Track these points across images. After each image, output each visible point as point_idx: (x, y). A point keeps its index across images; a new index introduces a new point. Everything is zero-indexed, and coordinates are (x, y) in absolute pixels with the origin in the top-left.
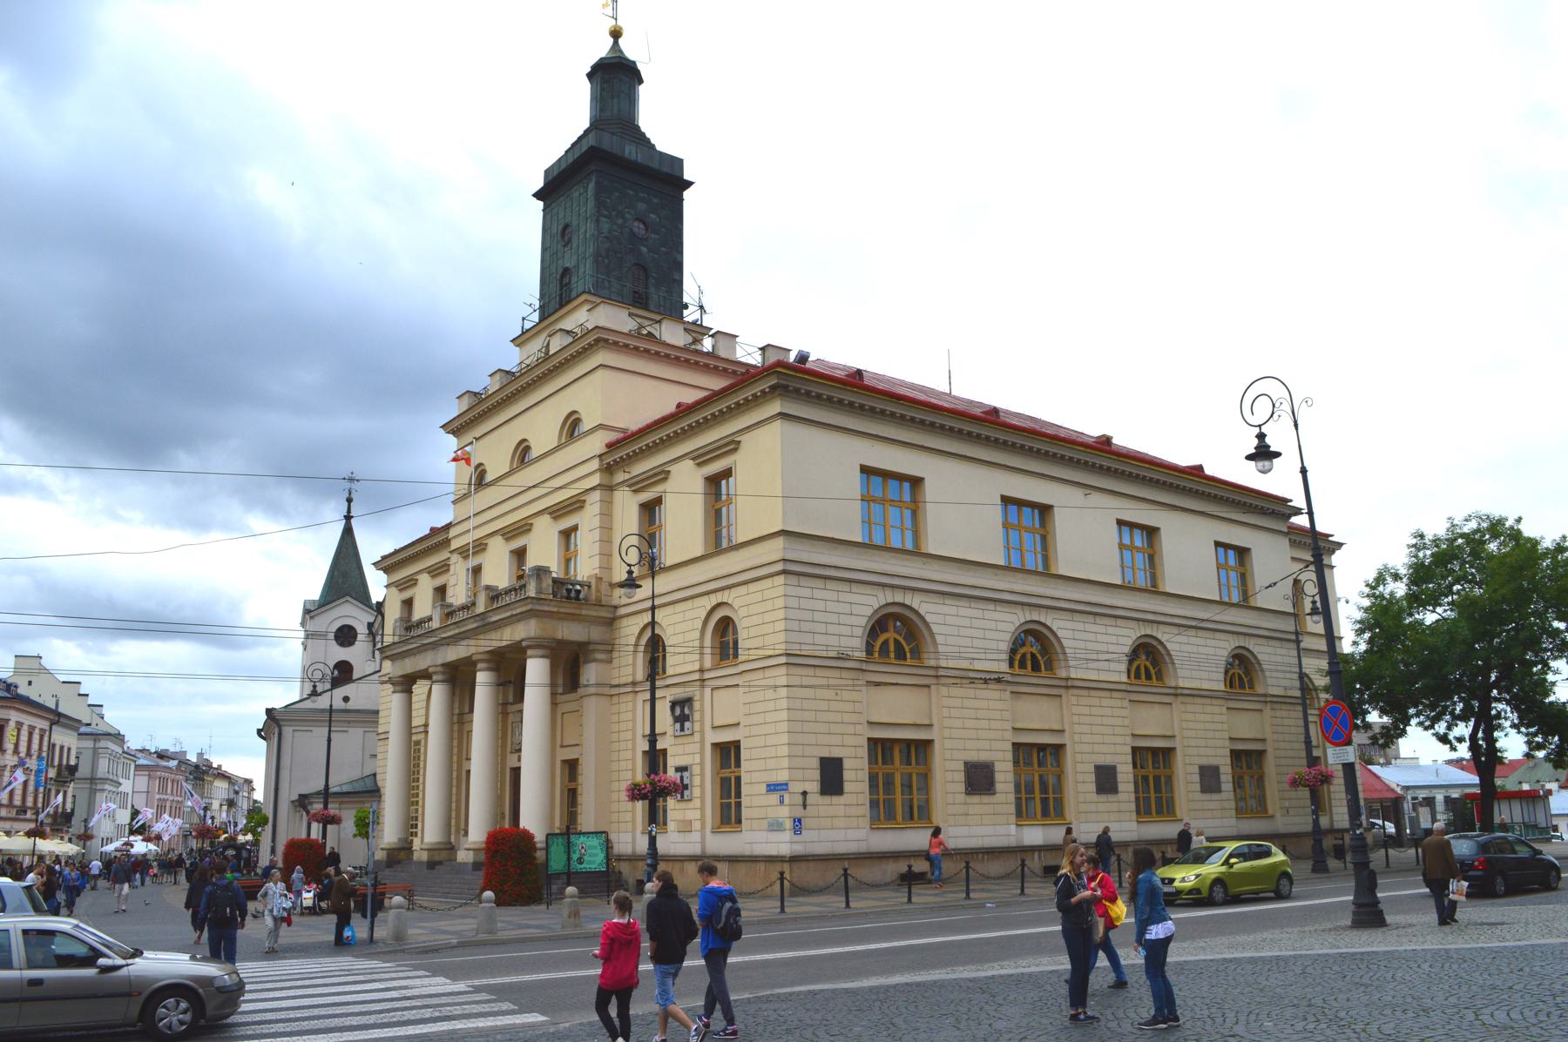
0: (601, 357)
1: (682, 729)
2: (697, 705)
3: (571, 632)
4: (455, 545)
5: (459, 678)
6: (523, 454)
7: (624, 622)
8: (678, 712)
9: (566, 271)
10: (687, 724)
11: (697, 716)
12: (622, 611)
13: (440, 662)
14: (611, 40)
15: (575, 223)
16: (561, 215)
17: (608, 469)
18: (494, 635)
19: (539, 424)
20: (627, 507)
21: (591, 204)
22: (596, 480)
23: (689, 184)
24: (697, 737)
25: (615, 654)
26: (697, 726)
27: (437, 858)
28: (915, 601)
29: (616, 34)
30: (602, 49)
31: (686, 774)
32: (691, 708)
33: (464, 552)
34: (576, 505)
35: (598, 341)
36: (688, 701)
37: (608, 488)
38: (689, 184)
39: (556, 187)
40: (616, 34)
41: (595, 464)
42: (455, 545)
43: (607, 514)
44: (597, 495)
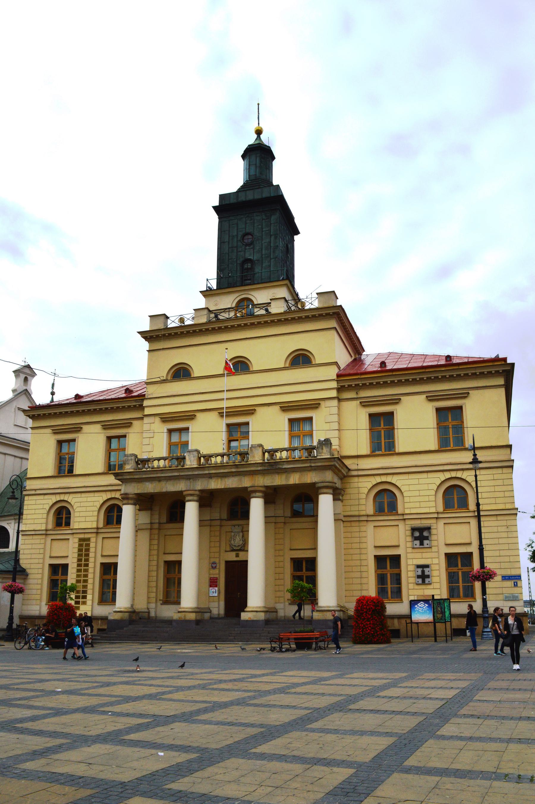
1: (422, 544)
2: (433, 531)
4: (147, 411)
8: (417, 534)
10: (426, 542)
11: (433, 537)
13: (199, 488)
14: (256, 136)
15: (257, 233)
17: (339, 390)
18: (284, 476)
19: (267, 350)
22: (334, 394)
24: (434, 549)
25: (344, 497)
26: (434, 543)
29: (259, 132)
30: (252, 139)
31: (426, 570)
32: (430, 533)
33: (165, 418)
34: (315, 405)
35: (334, 313)
36: (429, 529)
39: (228, 208)
40: (259, 132)
42: (147, 411)
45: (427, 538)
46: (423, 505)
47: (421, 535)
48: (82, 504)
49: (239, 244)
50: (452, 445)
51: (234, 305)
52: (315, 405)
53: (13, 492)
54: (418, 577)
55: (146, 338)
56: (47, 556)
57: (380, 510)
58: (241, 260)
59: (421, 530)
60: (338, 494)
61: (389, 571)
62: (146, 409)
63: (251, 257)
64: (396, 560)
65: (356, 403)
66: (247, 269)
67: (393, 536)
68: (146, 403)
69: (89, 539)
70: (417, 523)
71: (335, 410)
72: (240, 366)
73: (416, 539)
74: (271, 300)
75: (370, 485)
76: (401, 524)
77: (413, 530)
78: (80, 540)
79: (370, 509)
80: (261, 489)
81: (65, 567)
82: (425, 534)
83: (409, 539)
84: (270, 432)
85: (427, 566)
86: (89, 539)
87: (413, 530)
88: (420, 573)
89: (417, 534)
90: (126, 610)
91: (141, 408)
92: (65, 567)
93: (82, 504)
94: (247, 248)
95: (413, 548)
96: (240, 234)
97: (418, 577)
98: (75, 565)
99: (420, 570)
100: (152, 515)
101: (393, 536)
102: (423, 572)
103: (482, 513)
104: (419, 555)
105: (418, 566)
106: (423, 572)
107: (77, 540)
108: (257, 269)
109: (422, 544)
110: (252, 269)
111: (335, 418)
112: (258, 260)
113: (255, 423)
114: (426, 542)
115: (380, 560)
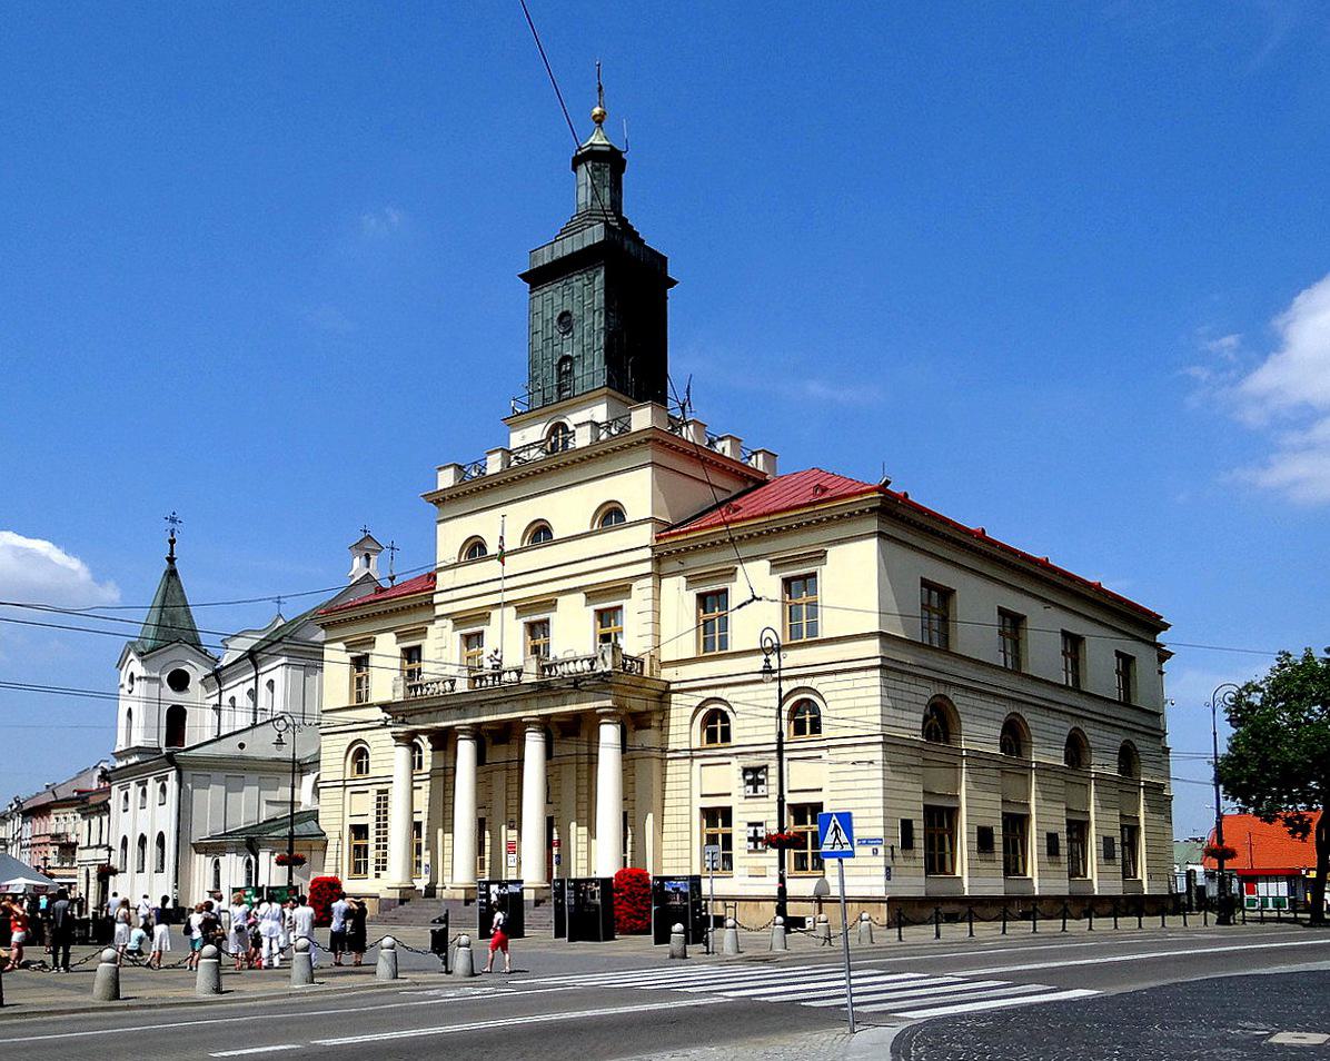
0: (647, 455)
1: (755, 790)
3: (636, 704)
4: (439, 610)
5: (498, 743)
6: (540, 533)
7: (674, 696)
9: (566, 359)
12: (673, 687)
15: (576, 313)
16: (558, 301)
17: (658, 560)
19: (569, 508)
20: (679, 598)
21: (599, 298)
22: (647, 567)
23: (672, 283)
27: (472, 896)
28: (950, 693)
32: (766, 774)
33: (459, 620)
34: (623, 589)
36: (766, 767)
37: (658, 576)
38: (672, 283)
41: (647, 553)
42: (439, 610)
43: (657, 599)
44: (649, 581)
45: (762, 782)
46: (760, 731)
47: (754, 776)
48: (380, 744)
49: (555, 331)
50: (805, 636)
51: (544, 437)
52: (623, 589)
53: (280, 736)
54: (750, 839)
55: (437, 503)
56: (347, 813)
57: (712, 737)
58: (558, 359)
59: (756, 770)
60: (632, 723)
61: (720, 830)
62: (437, 608)
63: (570, 353)
64: (726, 814)
65: (682, 580)
66: (566, 372)
67: (724, 780)
68: (437, 598)
69: (386, 791)
70: (753, 762)
71: (649, 593)
72: (540, 533)
73: (749, 783)
74: (575, 425)
75: (697, 702)
76: (733, 760)
77: (746, 771)
78: (379, 792)
79: (697, 738)
80: (537, 719)
81: (365, 827)
82: (761, 777)
83: (742, 783)
84: (573, 635)
85: (761, 824)
86: (386, 791)
87: (746, 771)
88: (752, 835)
89: (749, 777)
90: (396, 886)
91: (432, 605)
92: (365, 827)
93: (380, 744)
94: (566, 337)
95: (746, 797)
96: (558, 314)
97: (750, 839)
98: (374, 826)
99: (752, 829)
100: (445, 754)
101: (724, 780)
102: (756, 832)
103: (786, 747)
104: (753, 807)
105: (750, 824)
106: (756, 832)
107: (375, 792)
108: (578, 373)
109: (755, 790)
110: (571, 372)
111: (649, 605)
112: (578, 356)
113: (557, 620)
114: (760, 788)
115: (711, 815)
